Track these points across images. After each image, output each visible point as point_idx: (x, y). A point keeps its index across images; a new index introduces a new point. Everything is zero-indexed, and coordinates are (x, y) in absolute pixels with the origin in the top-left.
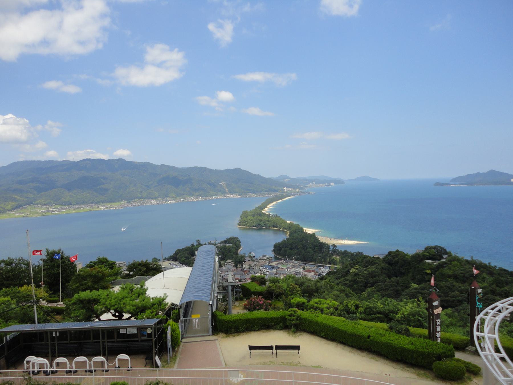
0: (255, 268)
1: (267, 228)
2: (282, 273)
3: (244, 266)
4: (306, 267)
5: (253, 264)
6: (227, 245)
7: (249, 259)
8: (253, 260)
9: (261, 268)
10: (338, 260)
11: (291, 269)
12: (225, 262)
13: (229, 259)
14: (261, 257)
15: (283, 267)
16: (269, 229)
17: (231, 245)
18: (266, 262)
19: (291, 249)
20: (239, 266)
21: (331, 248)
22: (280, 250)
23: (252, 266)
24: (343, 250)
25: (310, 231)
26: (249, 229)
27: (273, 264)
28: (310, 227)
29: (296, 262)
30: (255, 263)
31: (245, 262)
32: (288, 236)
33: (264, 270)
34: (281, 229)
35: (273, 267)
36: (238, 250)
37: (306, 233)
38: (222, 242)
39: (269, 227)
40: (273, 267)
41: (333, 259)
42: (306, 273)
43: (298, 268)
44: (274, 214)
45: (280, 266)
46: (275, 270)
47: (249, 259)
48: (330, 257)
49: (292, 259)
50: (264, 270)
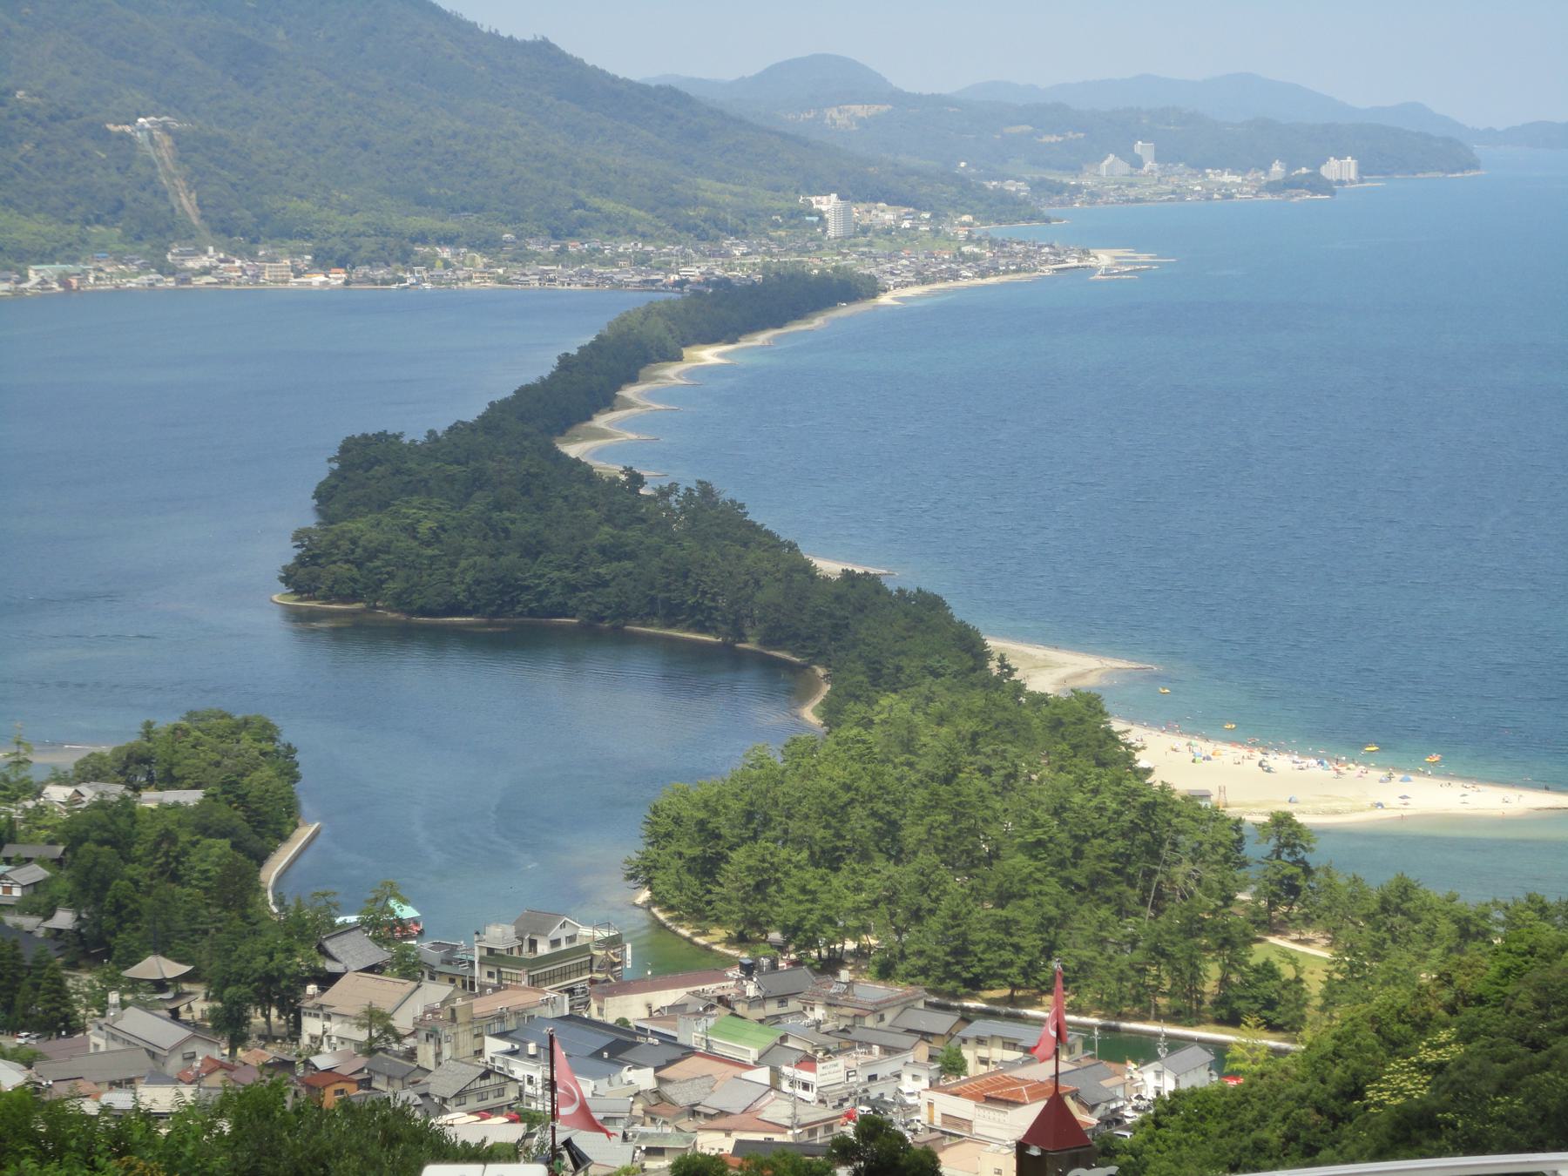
0: (426, 1055)
2: (713, 1102)
3: (311, 1026)
4: (969, 1054)
5: (412, 1004)
6: (150, 799)
7: (379, 955)
8: (411, 969)
9: (494, 1046)
10: (1315, 985)
11: (808, 1062)
12: (113, 982)
13: (163, 948)
14: (500, 935)
15: (722, 1047)
17: (191, 797)
18: (549, 992)
19: (830, 859)
20: (257, 1020)
21: (1255, 850)
22: (708, 867)
23: (402, 1022)
24: (1378, 881)
25: (1049, 670)
26: (404, 635)
27: (630, 1008)
29: (872, 990)
30: (434, 992)
31: (327, 980)
33: (520, 1069)
34: (750, 645)
35: (620, 1045)
36: (261, 858)
38: (90, 771)
39: (623, 613)
40: (620, 1045)
41: (1268, 971)
42: (963, 1108)
43: (889, 1050)
44: (687, 478)
45: (692, 1034)
46: (644, 1078)
47: (379, 955)
48: (1230, 943)
49: (831, 965)
50: (520, 1069)
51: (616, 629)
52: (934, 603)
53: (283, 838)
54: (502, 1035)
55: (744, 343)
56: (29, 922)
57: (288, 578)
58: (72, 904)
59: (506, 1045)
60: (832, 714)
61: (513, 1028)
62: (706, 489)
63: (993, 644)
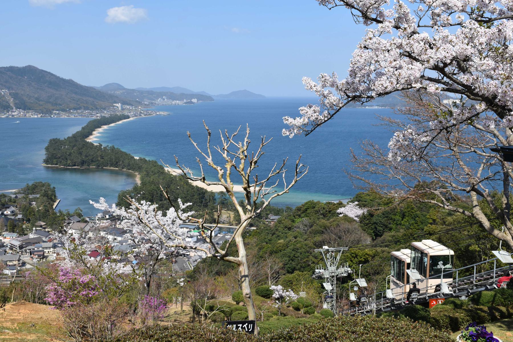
1: (100, 168)
9: (102, 234)
16: (103, 170)
21: (217, 197)
25: (175, 172)
28: (175, 164)
32: (138, 181)
37: (169, 174)
40: (123, 232)
44: (110, 145)
51: (102, 168)
52: (156, 162)
53: (55, 202)
54: (104, 231)
55: (118, 123)
56: (13, 217)
57: (46, 161)
58: (20, 214)
59: (105, 233)
60: (142, 179)
61: (104, 229)
62: (113, 147)
63: (166, 169)
